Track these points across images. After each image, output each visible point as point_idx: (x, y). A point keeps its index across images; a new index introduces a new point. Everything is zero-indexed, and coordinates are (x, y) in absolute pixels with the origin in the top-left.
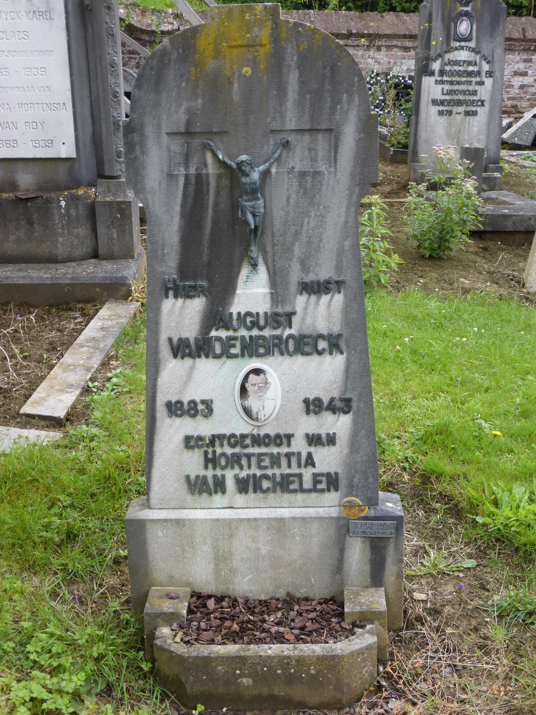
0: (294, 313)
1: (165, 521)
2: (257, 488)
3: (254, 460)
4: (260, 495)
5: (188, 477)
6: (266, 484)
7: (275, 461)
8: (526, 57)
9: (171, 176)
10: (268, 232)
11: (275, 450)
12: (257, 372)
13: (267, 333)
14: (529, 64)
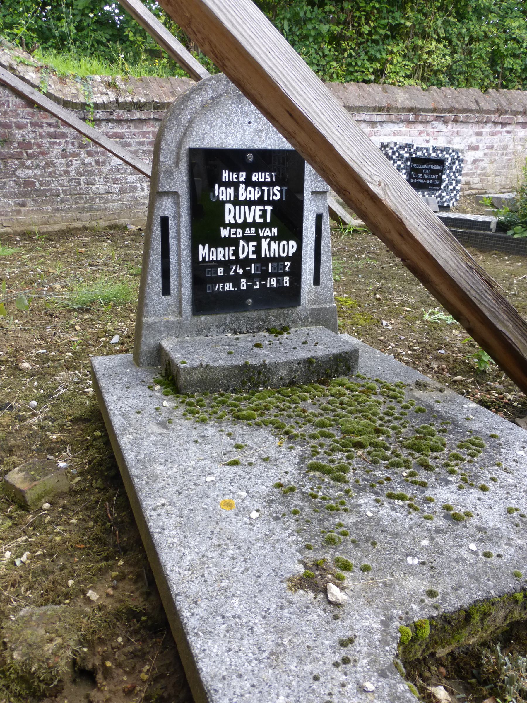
8: (477, 130)
14: (480, 138)
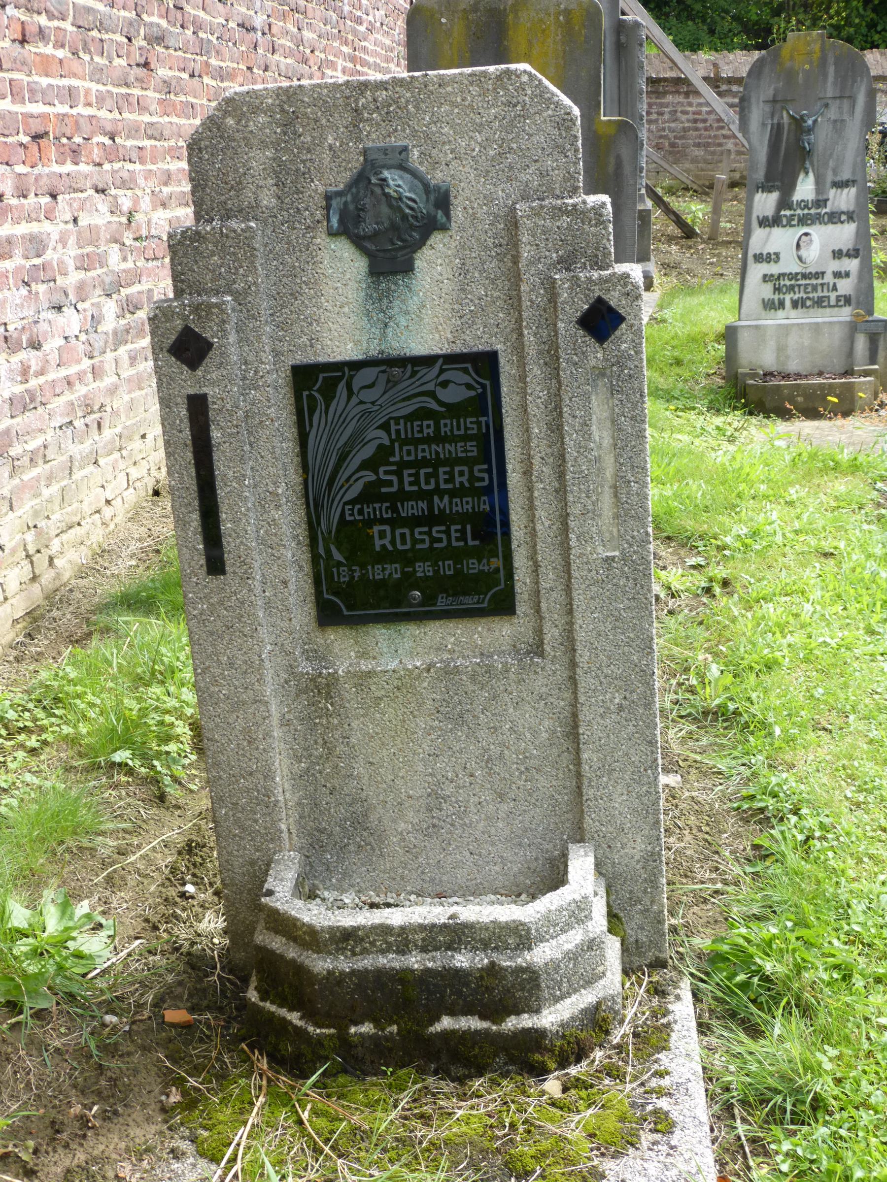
0: (828, 200)
1: (749, 326)
2: (803, 305)
3: (802, 288)
4: (805, 310)
5: (763, 300)
6: (808, 303)
7: (815, 288)
9: (764, 125)
10: (815, 154)
11: (814, 282)
12: (806, 234)
13: (813, 211)
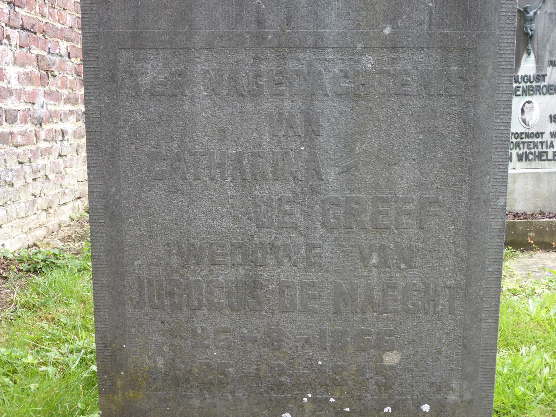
0: (546, 75)
2: (527, 159)
3: (526, 145)
4: (528, 162)
6: (531, 157)
7: (536, 146)
10: (536, 39)
11: (535, 140)
12: (529, 102)
13: (534, 84)
